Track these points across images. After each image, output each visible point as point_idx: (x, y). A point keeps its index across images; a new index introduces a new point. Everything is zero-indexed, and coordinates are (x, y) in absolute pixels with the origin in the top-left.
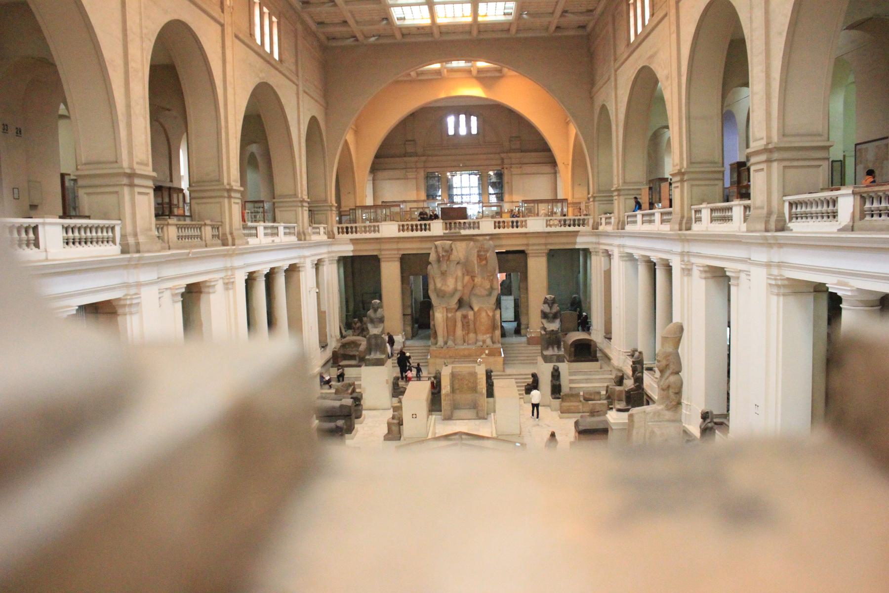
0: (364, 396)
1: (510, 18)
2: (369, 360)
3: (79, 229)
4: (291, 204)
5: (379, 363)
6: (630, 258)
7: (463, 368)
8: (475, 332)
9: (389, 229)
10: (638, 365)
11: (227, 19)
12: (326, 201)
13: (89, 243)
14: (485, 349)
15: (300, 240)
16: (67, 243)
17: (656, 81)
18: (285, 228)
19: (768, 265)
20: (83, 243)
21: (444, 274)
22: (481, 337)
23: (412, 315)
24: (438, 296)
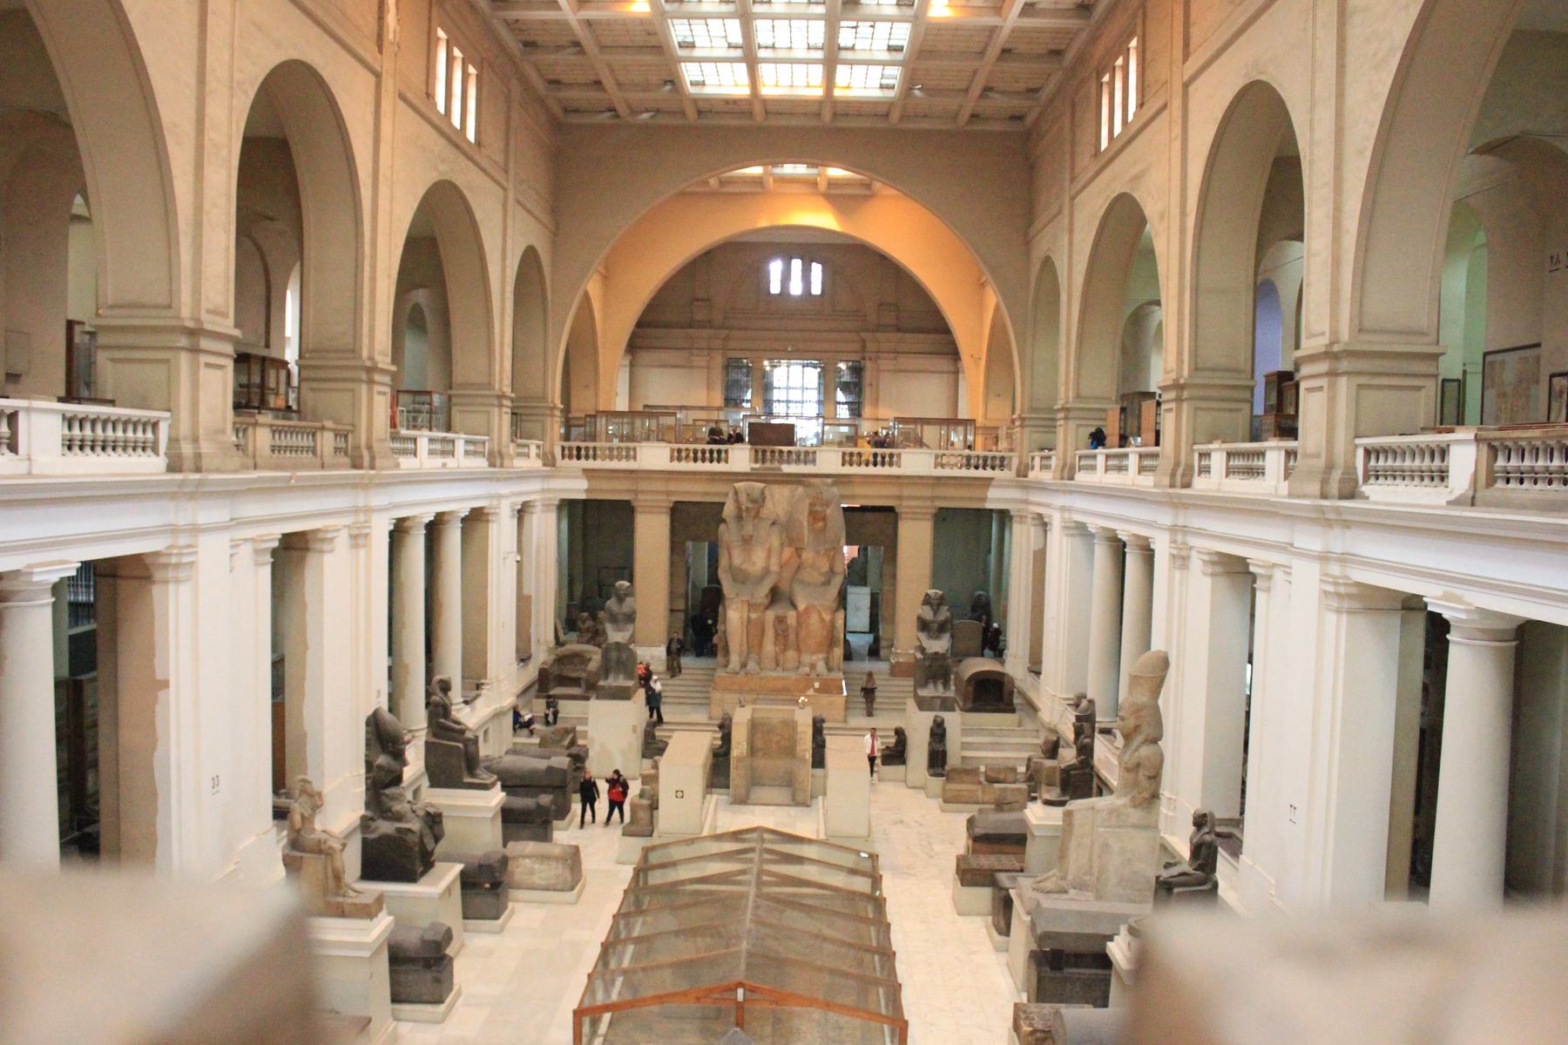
0: (591, 753)
1: (891, 94)
3: (94, 422)
4: (479, 400)
5: (623, 694)
6: (1081, 530)
7: (774, 712)
8: (798, 649)
9: (654, 456)
10: (1085, 724)
11: (386, 64)
12: (543, 398)
13: (109, 450)
15: (492, 465)
16: (70, 448)
17: (1142, 221)
18: (467, 442)
19: (1324, 558)
20: (98, 449)
21: (747, 541)
22: (806, 658)
23: (686, 611)
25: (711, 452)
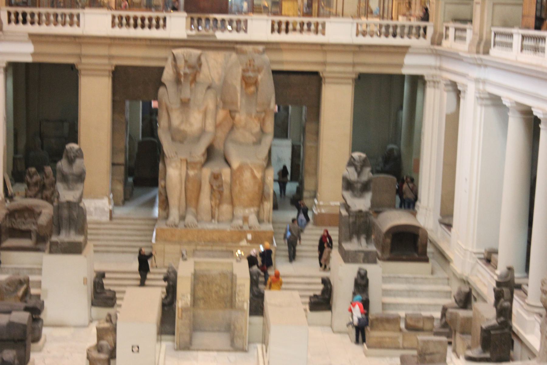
0: (46, 304)
2: (56, 243)
5: (75, 249)
6: (495, 101)
7: (214, 265)
8: (232, 203)
9: (96, 22)
10: (506, 288)
14: (245, 233)
21: (185, 104)
22: (240, 212)
23: (126, 165)
24: (173, 139)
25: (150, 19)
